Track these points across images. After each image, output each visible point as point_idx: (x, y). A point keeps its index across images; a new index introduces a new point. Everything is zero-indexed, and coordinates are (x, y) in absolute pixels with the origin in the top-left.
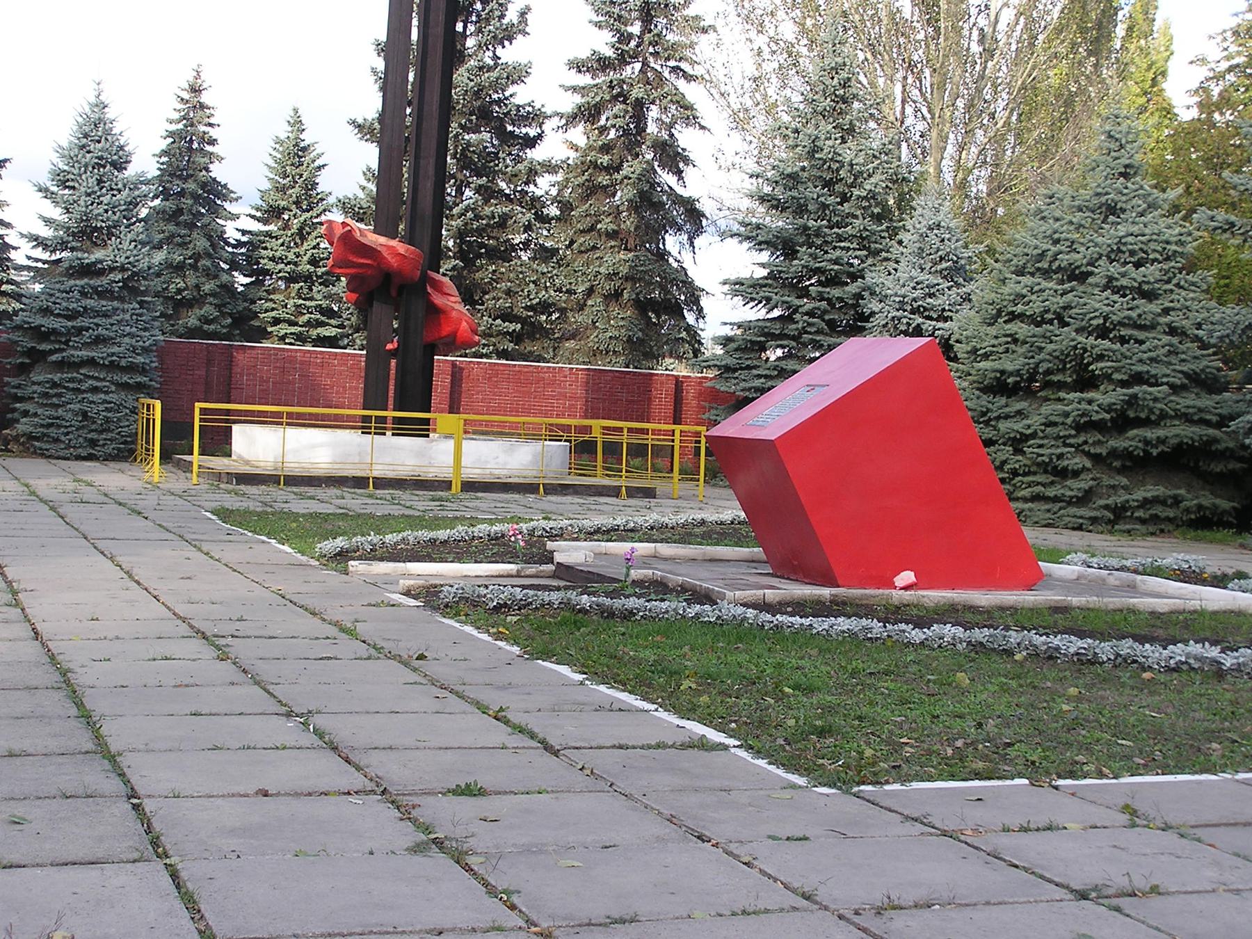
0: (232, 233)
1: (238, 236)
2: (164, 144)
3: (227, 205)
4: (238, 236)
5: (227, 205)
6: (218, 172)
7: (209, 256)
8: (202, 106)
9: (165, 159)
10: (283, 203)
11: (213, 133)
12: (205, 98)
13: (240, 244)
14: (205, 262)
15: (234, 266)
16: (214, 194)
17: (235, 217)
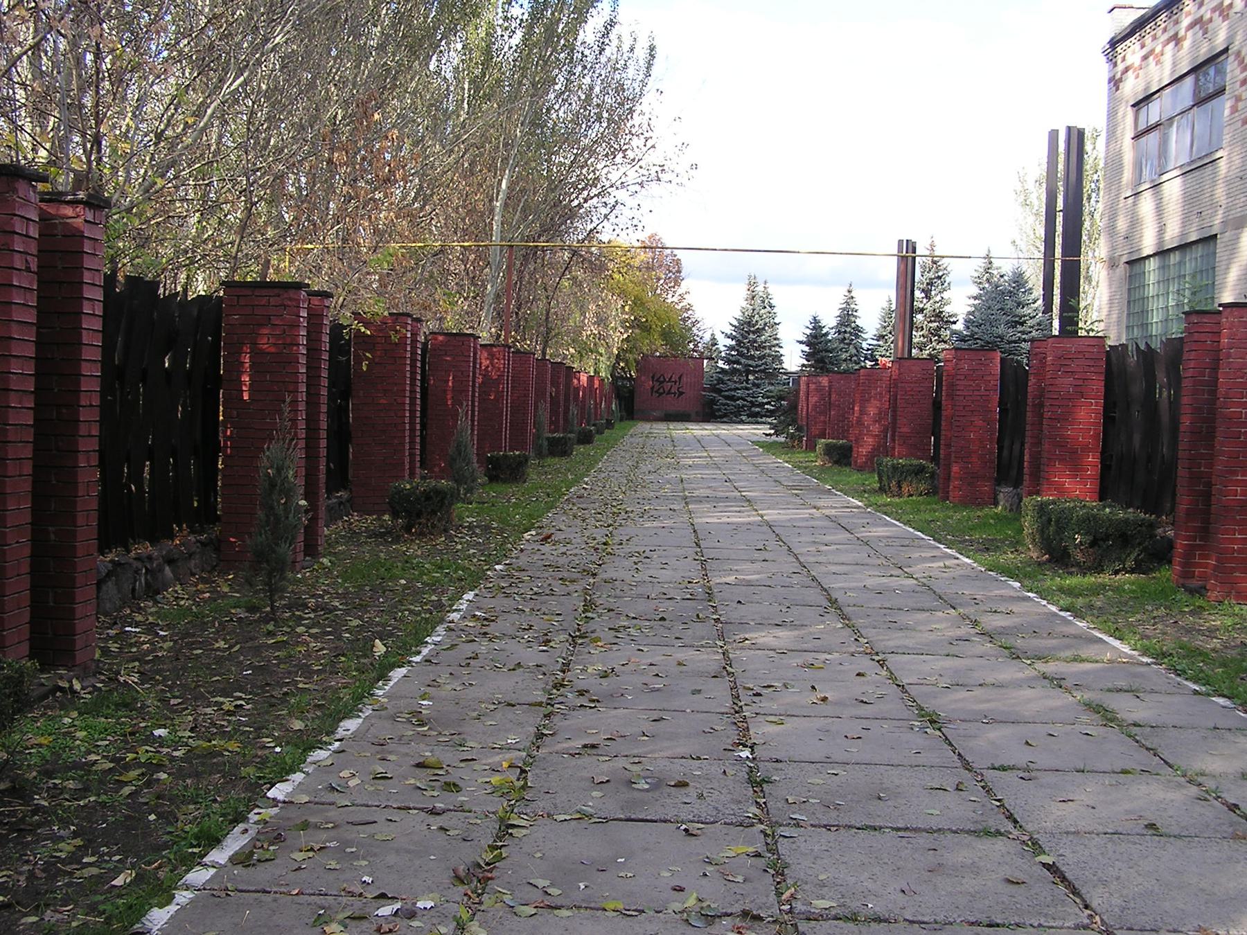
0: (865, 345)
1: (868, 346)
2: (838, 313)
3: (862, 335)
4: (868, 346)
5: (862, 335)
6: (858, 322)
7: (856, 355)
8: (852, 298)
9: (839, 318)
10: (885, 333)
11: (856, 307)
12: (852, 294)
13: (868, 350)
14: (855, 358)
15: (866, 358)
16: (858, 331)
17: (866, 340)
